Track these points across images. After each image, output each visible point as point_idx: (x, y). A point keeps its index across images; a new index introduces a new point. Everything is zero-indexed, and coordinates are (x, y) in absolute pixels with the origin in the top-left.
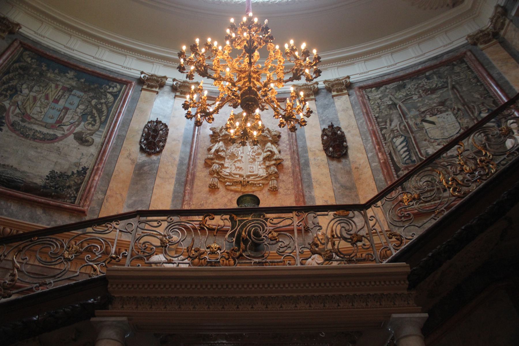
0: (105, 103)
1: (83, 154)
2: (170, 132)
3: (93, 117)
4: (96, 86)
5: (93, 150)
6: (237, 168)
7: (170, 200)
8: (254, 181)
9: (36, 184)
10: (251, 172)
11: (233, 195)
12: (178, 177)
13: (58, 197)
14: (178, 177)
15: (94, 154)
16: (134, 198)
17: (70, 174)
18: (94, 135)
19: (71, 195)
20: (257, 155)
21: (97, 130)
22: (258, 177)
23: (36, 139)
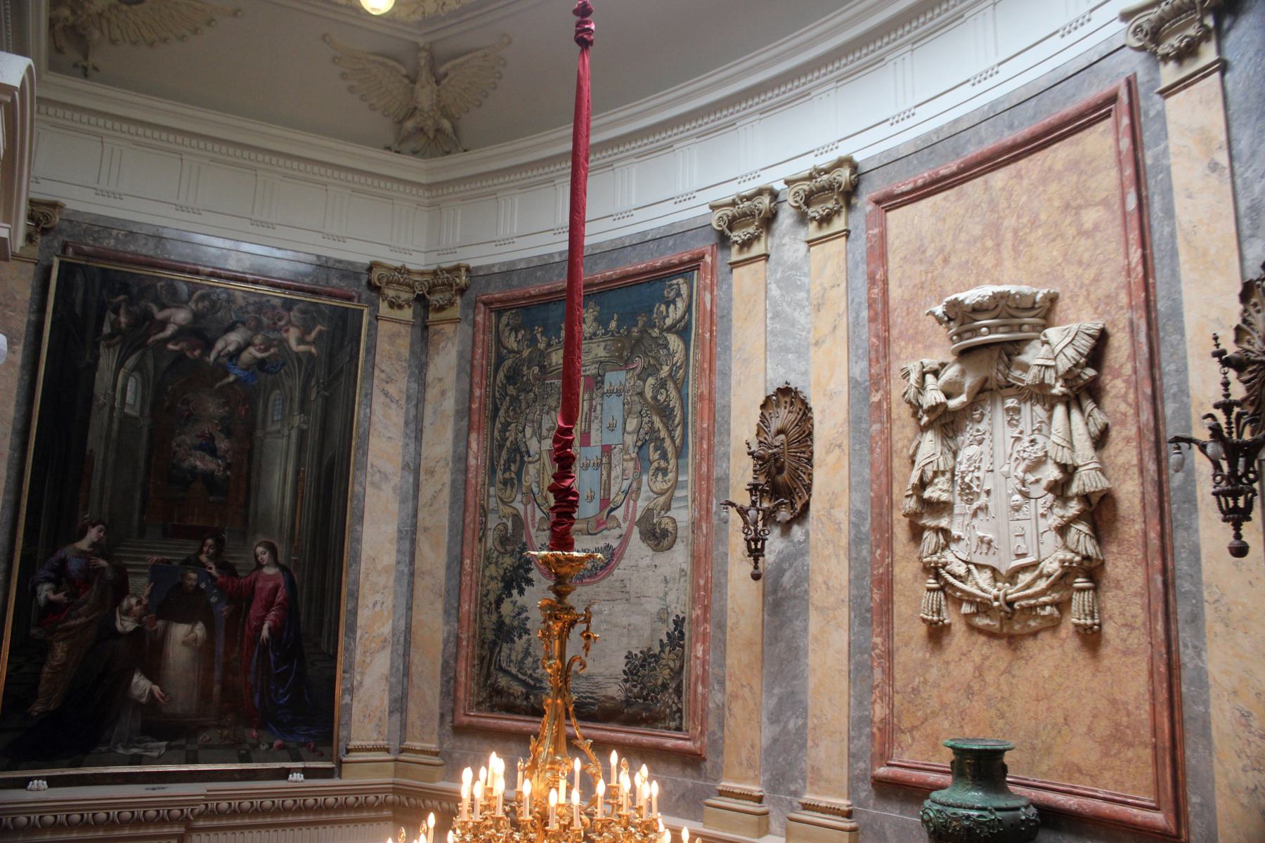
0: (670, 375)
1: (666, 581)
2: (816, 415)
3: (660, 447)
4: (640, 323)
5: (679, 556)
7: (845, 684)
9: (613, 698)
10: (1019, 556)
11: (985, 650)
12: (855, 592)
13: (652, 720)
14: (855, 592)
15: (684, 566)
16: (776, 691)
17: (657, 650)
18: (674, 505)
19: (670, 707)
20: (1029, 469)
21: (676, 485)
22: (1040, 576)
23: (583, 576)
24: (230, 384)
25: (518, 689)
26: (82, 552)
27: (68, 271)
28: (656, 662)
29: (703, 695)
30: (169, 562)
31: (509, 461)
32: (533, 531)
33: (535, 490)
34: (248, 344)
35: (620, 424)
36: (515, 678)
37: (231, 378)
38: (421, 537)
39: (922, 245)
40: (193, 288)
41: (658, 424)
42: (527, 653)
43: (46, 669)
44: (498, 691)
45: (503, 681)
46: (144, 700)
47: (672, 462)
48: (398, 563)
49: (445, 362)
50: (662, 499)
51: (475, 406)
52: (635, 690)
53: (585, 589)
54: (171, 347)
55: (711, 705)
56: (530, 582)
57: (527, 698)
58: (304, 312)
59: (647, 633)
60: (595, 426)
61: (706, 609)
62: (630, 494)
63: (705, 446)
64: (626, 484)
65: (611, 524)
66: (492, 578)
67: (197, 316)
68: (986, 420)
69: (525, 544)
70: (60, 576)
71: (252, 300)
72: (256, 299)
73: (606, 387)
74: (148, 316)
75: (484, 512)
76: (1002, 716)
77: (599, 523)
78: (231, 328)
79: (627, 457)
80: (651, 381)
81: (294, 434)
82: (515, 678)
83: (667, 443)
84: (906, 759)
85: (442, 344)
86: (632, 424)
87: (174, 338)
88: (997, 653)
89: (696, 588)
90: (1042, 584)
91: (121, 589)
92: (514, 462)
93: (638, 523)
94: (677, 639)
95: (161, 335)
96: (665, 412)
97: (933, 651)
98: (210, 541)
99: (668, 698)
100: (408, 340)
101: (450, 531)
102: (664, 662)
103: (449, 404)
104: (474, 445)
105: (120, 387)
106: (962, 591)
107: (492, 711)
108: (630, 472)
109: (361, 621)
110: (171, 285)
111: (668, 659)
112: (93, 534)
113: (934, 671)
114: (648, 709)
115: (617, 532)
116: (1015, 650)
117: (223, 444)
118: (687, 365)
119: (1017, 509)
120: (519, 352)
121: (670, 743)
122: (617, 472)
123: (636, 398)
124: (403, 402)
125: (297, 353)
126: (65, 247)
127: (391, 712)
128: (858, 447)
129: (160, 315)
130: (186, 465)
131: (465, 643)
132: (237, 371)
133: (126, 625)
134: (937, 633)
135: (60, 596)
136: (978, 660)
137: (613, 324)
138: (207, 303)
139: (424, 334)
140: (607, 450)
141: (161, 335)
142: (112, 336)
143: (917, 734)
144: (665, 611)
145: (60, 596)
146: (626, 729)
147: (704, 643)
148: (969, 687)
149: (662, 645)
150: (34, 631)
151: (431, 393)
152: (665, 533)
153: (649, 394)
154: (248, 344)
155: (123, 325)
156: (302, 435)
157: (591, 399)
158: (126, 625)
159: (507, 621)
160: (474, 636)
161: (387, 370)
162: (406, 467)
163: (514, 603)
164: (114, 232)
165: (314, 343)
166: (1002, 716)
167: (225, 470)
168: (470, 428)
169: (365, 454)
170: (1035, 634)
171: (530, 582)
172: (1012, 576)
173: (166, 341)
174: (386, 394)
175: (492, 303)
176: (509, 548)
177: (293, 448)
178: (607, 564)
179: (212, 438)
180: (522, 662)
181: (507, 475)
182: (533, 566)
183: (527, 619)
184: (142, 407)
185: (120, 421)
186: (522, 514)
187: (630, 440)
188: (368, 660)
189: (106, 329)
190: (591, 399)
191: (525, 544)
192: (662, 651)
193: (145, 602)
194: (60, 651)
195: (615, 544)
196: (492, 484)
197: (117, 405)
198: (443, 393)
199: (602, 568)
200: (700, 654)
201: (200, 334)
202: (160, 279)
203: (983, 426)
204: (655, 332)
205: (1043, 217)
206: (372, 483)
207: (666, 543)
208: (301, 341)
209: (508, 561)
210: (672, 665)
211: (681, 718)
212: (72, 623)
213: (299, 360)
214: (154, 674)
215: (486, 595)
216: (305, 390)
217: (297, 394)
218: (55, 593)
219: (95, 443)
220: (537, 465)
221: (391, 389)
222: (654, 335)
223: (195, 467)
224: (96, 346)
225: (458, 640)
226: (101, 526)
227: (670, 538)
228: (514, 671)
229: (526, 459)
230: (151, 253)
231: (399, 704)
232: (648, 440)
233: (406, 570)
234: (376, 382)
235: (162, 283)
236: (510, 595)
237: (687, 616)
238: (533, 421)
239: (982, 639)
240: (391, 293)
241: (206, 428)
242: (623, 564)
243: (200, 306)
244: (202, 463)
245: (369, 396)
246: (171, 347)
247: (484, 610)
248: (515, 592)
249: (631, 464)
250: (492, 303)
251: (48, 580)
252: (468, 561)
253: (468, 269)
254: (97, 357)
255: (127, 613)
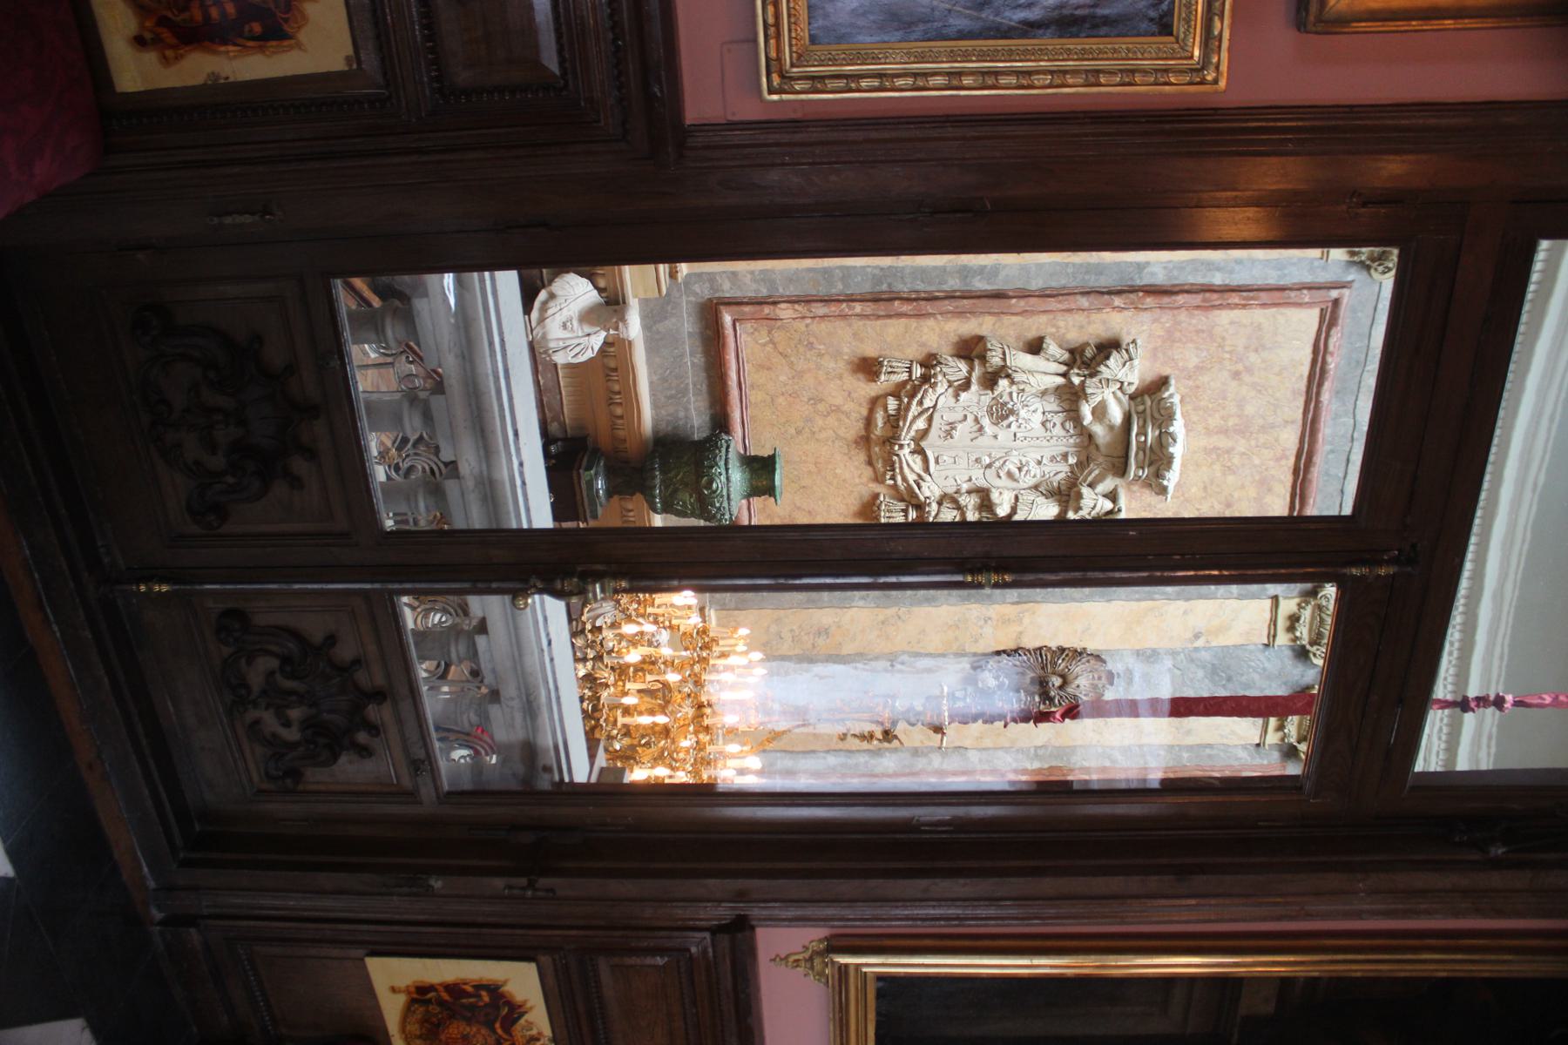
6: (952, 426)
8: (901, 468)
39: (1264, 347)
68: (1063, 433)
76: (799, 432)
84: (744, 338)
88: (854, 428)
90: (911, 478)
97: (850, 363)
106: (909, 403)
113: (832, 365)
116: (856, 442)
119: (978, 460)
128: (1070, 270)
134: (869, 368)
136: (846, 408)
143: (769, 348)
148: (821, 400)
166: (799, 432)
170: (870, 463)
172: (919, 451)
203: (1058, 431)
205: (1230, 478)
239: (865, 412)
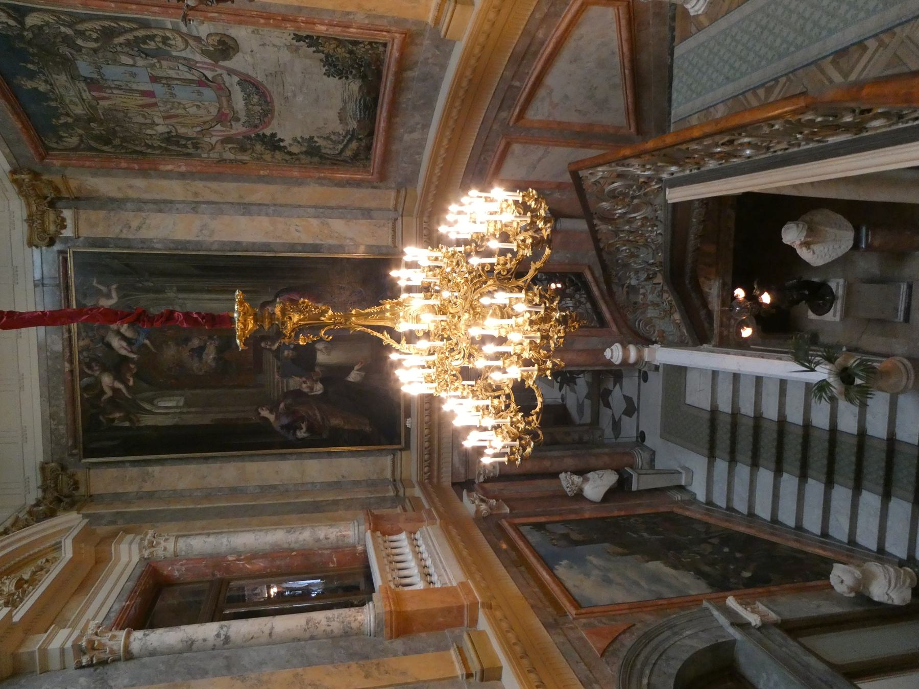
0: (70, 26)
5: (241, 33)
9: (360, 87)
15: (249, 30)
17: (322, 56)
18: (195, 33)
19: (367, 50)
24: (151, 342)
25: (354, 145)
26: (277, 418)
27: (88, 453)
28: (332, 56)
29: (358, 28)
30: (278, 368)
31: (177, 144)
32: (233, 132)
33: (199, 129)
34: (118, 333)
35: (129, 69)
36: (346, 146)
37: (147, 342)
38: (246, 201)
40: (83, 374)
41: (121, 39)
42: (328, 138)
43: (346, 427)
44: (355, 157)
45: (348, 153)
46: (363, 374)
47: (155, 32)
48: (267, 215)
49: (104, 186)
50: (191, 42)
51: (136, 167)
52: (354, 72)
53: (275, 100)
54: (131, 383)
55: (366, 21)
56: (273, 135)
57: (361, 139)
58: (85, 296)
59: (308, 62)
60: (134, 87)
61: (285, 19)
62: (191, 65)
63: (134, 7)
64: (181, 67)
65: (219, 79)
66: (273, 157)
67: (105, 369)
69: (244, 137)
70: (292, 427)
71: (84, 334)
72: (82, 330)
73: (95, 76)
74: (111, 400)
75: (222, 161)
77: (220, 88)
78: (109, 346)
79: (158, 65)
80: (79, 42)
81: (181, 296)
82: (346, 146)
83: (137, 34)
85: (88, 187)
86: (125, 59)
87: (124, 382)
89: (266, 25)
91: (298, 394)
92: (178, 142)
93: (216, 61)
94: (313, 41)
95: (124, 391)
96: (108, 34)
98: (263, 345)
99: (360, 50)
100: (91, 212)
101: (240, 182)
102: (331, 52)
103: (139, 183)
104: (169, 167)
105: (166, 410)
107: (370, 159)
108: (171, 64)
109: (310, 241)
110: (85, 389)
111: (330, 48)
112: (265, 413)
114: (369, 65)
115: (226, 77)
117: (195, 343)
118: (54, 11)
120: (81, 136)
121: (396, 54)
122: (172, 73)
123: (100, 55)
124: (144, 214)
125: (119, 298)
126: (72, 455)
127: (371, 218)
129: (109, 393)
130: (213, 364)
131: (322, 175)
132: (141, 339)
133: (319, 388)
135: (304, 426)
137: (31, 66)
138: (93, 364)
139: (82, 200)
140: (154, 79)
141: (124, 391)
142: (131, 420)
144: (289, 47)
145: (304, 426)
146: (384, 79)
147: (314, 24)
149: (317, 51)
150: (324, 436)
151: (132, 194)
152: (221, 42)
153: (94, 45)
154: (118, 333)
155: (122, 414)
156: (181, 290)
157: (111, 88)
158: (319, 388)
159: (304, 149)
160: (317, 169)
161: (120, 227)
162: (195, 210)
163: (290, 145)
164: (53, 427)
165: (108, 286)
167: (213, 339)
168: (156, 170)
169: (189, 242)
171: (273, 135)
173: (127, 387)
174: (139, 228)
175: (40, 154)
176: (248, 146)
177: (192, 296)
178: (254, 85)
179: (192, 350)
180: (334, 142)
181: (190, 146)
182: (261, 133)
183: (302, 137)
184: (177, 396)
185: (190, 407)
186: (219, 138)
187: (141, 62)
188: (336, 235)
189: (127, 424)
190: (111, 88)
191: (244, 137)
192: (323, 52)
193: (304, 379)
194: (335, 422)
195: (236, 79)
196: (200, 156)
197: (178, 411)
198: (131, 187)
199: (257, 88)
200: (324, 28)
201: (118, 366)
202: (81, 396)
204: (28, 35)
206: (210, 236)
207: (230, 42)
208: (108, 296)
209: (259, 147)
210: (333, 46)
211: (376, 43)
212: (319, 417)
213: (125, 296)
214: (348, 369)
215: (287, 161)
216: (147, 290)
217: (152, 296)
218: (302, 428)
219: (206, 420)
220: (178, 127)
221: (135, 224)
222: (31, 35)
223: (214, 359)
224: (140, 428)
225: (319, 178)
226: (260, 410)
227: (226, 39)
228: (341, 146)
229: (174, 134)
230: (63, 402)
231: (367, 213)
232: (137, 47)
233: (272, 208)
234: (130, 236)
235: (86, 396)
236: (285, 147)
237: (292, 33)
238: (140, 129)
240: (52, 228)
241: (185, 355)
242: (251, 73)
243: (97, 368)
244: (210, 354)
245: (143, 241)
246: (131, 383)
247: (297, 162)
248: (282, 144)
249: (164, 63)
250: (40, 154)
251: (294, 434)
252: (262, 172)
253: (14, 172)
254: (148, 427)
255: (312, 389)
